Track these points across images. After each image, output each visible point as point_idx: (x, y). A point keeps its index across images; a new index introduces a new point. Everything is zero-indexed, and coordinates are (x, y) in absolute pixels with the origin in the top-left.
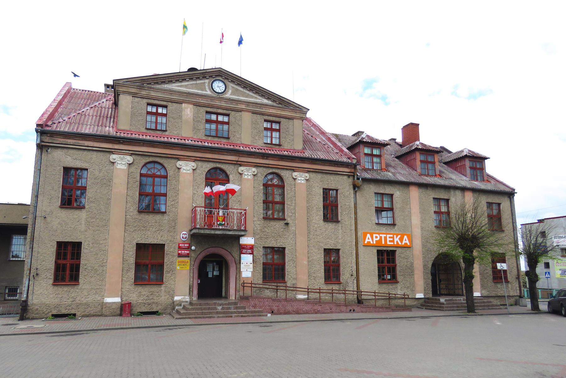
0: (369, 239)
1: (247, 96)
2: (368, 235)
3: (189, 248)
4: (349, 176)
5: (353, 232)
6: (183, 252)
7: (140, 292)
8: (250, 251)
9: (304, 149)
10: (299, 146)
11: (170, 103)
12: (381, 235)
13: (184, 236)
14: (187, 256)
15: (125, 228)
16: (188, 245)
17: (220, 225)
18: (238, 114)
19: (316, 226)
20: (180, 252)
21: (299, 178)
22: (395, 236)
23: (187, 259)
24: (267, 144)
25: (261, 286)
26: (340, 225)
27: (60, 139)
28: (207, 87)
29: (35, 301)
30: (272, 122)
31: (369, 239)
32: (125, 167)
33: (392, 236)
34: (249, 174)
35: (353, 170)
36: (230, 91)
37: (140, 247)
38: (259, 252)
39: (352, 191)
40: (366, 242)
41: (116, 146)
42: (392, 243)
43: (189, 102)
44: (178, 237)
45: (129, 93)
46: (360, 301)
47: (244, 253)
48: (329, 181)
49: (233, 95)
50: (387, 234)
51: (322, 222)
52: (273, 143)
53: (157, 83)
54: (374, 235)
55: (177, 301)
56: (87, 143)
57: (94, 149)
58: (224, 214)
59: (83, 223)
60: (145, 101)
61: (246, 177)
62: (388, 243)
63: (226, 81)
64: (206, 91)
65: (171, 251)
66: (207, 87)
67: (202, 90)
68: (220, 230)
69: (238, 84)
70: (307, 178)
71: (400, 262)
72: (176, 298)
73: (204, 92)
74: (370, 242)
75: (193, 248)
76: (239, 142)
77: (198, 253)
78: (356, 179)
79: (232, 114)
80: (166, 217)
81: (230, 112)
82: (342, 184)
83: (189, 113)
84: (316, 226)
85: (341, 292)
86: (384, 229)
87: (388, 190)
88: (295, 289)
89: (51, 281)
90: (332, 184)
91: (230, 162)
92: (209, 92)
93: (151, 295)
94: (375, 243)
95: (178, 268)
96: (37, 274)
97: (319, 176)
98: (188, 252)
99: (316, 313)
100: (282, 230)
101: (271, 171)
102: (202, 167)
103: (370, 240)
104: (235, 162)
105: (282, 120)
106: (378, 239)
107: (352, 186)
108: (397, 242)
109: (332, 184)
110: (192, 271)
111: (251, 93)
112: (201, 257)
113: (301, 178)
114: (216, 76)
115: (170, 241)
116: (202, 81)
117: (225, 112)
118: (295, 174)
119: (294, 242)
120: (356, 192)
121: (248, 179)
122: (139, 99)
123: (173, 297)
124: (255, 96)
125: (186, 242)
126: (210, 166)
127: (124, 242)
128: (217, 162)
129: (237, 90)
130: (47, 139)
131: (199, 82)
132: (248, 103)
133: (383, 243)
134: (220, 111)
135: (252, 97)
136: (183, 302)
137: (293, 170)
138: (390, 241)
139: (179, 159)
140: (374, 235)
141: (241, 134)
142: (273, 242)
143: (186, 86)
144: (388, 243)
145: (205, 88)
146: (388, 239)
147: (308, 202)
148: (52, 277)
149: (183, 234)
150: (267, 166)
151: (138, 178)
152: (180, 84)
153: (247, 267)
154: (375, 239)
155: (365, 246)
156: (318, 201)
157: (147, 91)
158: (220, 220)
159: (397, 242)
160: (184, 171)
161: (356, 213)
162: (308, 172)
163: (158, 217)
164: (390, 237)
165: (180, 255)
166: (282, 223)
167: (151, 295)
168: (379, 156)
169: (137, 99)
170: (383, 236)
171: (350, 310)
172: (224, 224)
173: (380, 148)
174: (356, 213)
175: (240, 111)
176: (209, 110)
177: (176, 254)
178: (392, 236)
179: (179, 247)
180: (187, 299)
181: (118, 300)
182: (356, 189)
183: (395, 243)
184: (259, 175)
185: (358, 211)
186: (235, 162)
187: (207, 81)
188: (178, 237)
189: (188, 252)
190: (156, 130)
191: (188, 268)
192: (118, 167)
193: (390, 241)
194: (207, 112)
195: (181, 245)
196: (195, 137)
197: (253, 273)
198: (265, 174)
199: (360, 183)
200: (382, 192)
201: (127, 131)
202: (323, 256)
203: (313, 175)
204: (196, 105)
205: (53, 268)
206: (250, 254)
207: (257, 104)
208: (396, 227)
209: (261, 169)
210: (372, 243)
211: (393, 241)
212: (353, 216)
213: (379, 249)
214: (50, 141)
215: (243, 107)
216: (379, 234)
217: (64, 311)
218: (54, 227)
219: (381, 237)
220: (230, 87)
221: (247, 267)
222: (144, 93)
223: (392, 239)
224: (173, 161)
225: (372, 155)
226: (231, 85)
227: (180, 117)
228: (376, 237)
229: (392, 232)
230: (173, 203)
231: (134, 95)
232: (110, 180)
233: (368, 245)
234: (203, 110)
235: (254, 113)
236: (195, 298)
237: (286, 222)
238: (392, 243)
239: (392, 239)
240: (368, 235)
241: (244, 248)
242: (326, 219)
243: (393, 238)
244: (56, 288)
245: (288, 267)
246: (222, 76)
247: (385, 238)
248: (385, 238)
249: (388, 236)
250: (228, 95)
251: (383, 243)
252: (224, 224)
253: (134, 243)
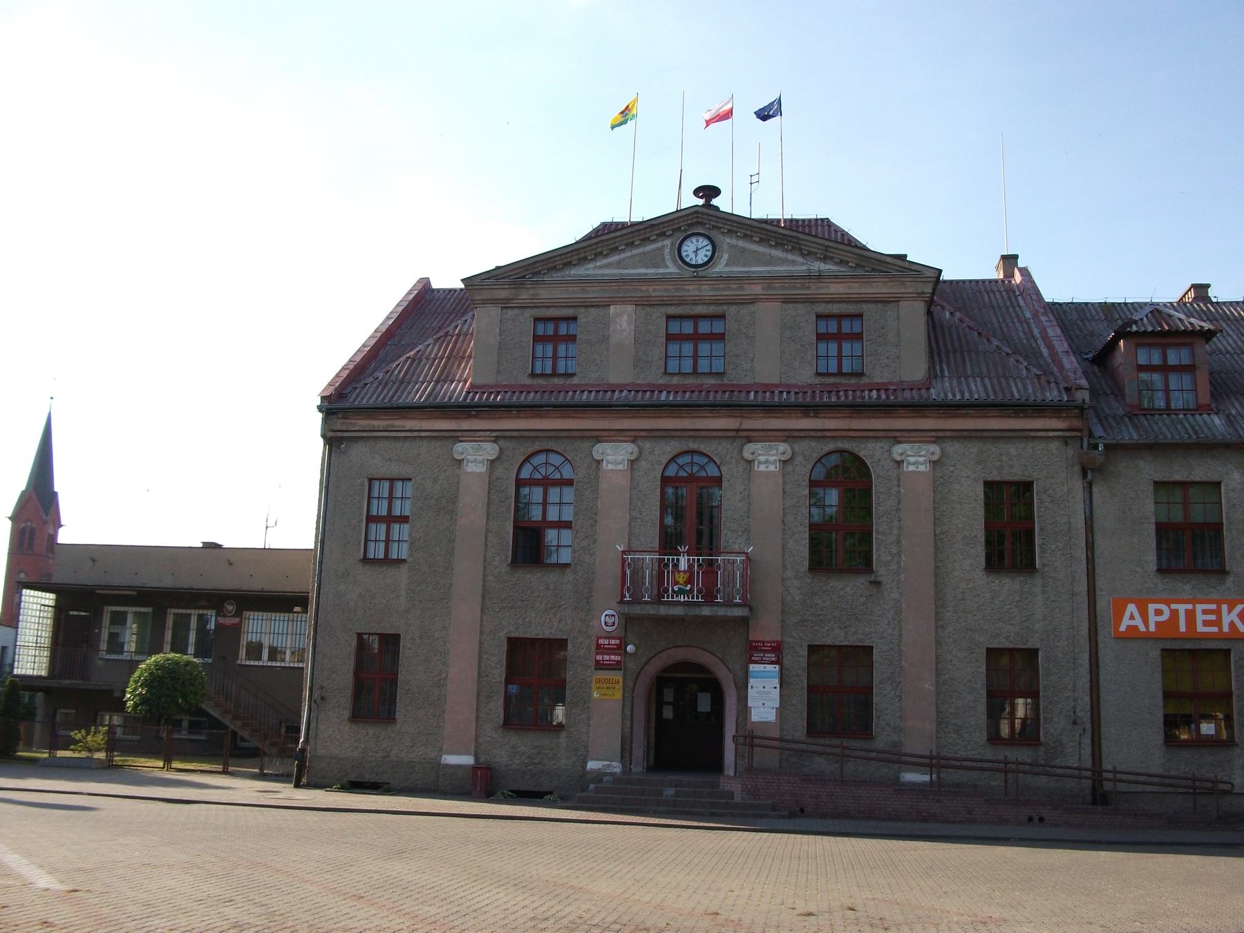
0: (1132, 617)
1: (770, 261)
2: (1131, 608)
3: (621, 648)
4: (1065, 441)
5: (1083, 599)
6: (607, 657)
7: (514, 747)
8: (772, 657)
9: (932, 376)
10: (914, 367)
11: (583, 310)
12: (1173, 606)
13: (610, 621)
14: (616, 666)
15: (483, 603)
16: (618, 642)
17: (681, 592)
18: (745, 311)
19: (963, 585)
20: (599, 658)
21: (912, 459)
22: (1224, 607)
23: (617, 676)
24: (828, 375)
25: (803, 746)
26: (1038, 581)
27: (360, 422)
28: (667, 257)
29: (321, 752)
30: (840, 317)
31: (1132, 617)
32: (482, 469)
33: (1213, 607)
34: (772, 458)
35: (1076, 423)
36: (726, 256)
37: (515, 645)
38: (798, 659)
39: (1078, 485)
40: (1123, 628)
41: (465, 425)
42: (1215, 629)
43: (623, 301)
44: (595, 623)
45: (494, 302)
46: (1100, 798)
47: (756, 662)
48: (1004, 458)
49: (734, 264)
50: (1194, 602)
51: (980, 577)
52: (845, 370)
53: (554, 268)
54: (1152, 607)
55: (592, 771)
56: (408, 424)
57: (423, 434)
58: (691, 566)
59: (403, 593)
60: (529, 313)
61: (762, 468)
62: (1200, 628)
63: (713, 234)
64: (667, 267)
65: (579, 653)
66: (667, 257)
67: (655, 266)
68: (679, 603)
69: (745, 236)
70: (935, 458)
71: (411, 671)
72: (592, 765)
73: (661, 271)
74: (1136, 627)
75: (630, 648)
76: (748, 381)
77: (643, 660)
78: (1085, 446)
79: (731, 311)
80: (569, 576)
81: (725, 307)
82: (1046, 464)
83: (624, 325)
84: (963, 585)
85: (1037, 769)
86: (1187, 587)
87: (1200, 470)
88: (899, 758)
89: (347, 714)
90: (1011, 466)
91: (720, 434)
92: (672, 269)
93: (539, 753)
94: (1152, 628)
95: (595, 695)
96: (322, 698)
97: (974, 448)
98: (618, 658)
99: (925, 820)
100: (863, 599)
101: (830, 446)
102: (652, 452)
103: (1138, 622)
104: (733, 434)
105: (866, 309)
106: (1165, 617)
107: (1077, 468)
108: (1232, 624)
109: (1011, 466)
110: (628, 704)
111: (777, 253)
112: (653, 669)
113: (916, 459)
114: (689, 225)
115: (580, 632)
116: (659, 245)
117: (712, 310)
118: (898, 450)
119: (896, 633)
120: (1090, 484)
121: (768, 474)
122: (516, 311)
123: (585, 763)
124: (790, 257)
125: (614, 634)
126: (672, 447)
127: (481, 633)
128: (690, 437)
129: (743, 250)
130: (339, 424)
131: (649, 248)
132: (768, 279)
133: (1183, 628)
134: (699, 310)
135: (783, 261)
136: (606, 774)
137: (896, 437)
138: (1206, 623)
139: (598, 440)
140: (1152, 607)
141: (753, 360)
142: (837, 631)
143: (618, 264)
144: (1200, 628)
145: (663, 259)
146: (1200, 618)
147: (936, 521)
148: (349, 705)
149: (607, 618)
150: (819, 434)
151: (512, 491)
152: (605, 261)
153: (764, 697)
154: (1153, 619)
155: (1121, 638)
156: (969, 517)
157: (531, 292)
158: (681, 580)
159: (1232, 624)
160: (610, 467)
161: (1090, 546)
162: (937, 440)
163: (552, 577)
164: (1205, 612)
165: (599, 666)
166: (861, 581)
167: (539, 753)
168: (1190, 369)
169: (510, 312)
170: (1182, 608)
171: (1030, 819)
172: (691, 591)
173: (1191, 345)
174: (1090, 546)
175: (753, 301)
176: (673, 310)
177: (592, 663)
178: (1213, 607)
179: (598, 646)
180: (616, 767)
181: (468, 760)
182: (1089, 476)
183: (1226, 629)
184: (799, 459)
185: (1098, 539)
186: (733, 434)
187: (668, 242)
188: (595, 623)
189: (618, 658)
190: (554, 374)
191: (618, 695)
192: (468, 470)
193: (1206, 623)
194: (669, 317)
195: (601, 641)
196: (640, 381)
197: (781, 711)
198: (816, 456)
199: (1101, 459)
200: (1178, 477)
201: (491, 387)
202: (983, 669)
203: (953, 447)
204: (643, 303)
205: (351, 686)
206: (772, 663)
207: (791, 277)
208: (1229, 581)
209: (801, 446)
210: (1142, 629)
211: (1218, 623)
212: (1081, 554)
213: (1169, 646)
214: (344, 428)
215: (757, 289)
216: (1167, 602)
217: (369, 777)
218: (352, 604)
219: (1174, 613)
220: (725, 247)
221: (764, 697)
222: (525, 296)
223: (1213, 617)
224: (585, 445)
225: (1165, 369)
226: (726, 241)
227: (605, 339)
228: (1158, 612)
229: (1214, 597)
230: (585, 543)
231: (505, 304)
232: (454, 500)
233: (1133, 635)
234: (658, 314)
235: (787, 301)
236: (638, 768)
237: (873, 578)
238: (1215, 629)
239: (1213, 617)
240: (1131, 608)
241: (756, 649)
242: (996, 561)
243: (1218, 612)
244: (354, 727)
245: (880, 699)
246: (703, 224)
247: (1191, 615)
248: (1191, 615)
249: (1199, 607)
250: (720, 268)
251: (1183, 628)
252: (691, 591)
253: (502, 635)
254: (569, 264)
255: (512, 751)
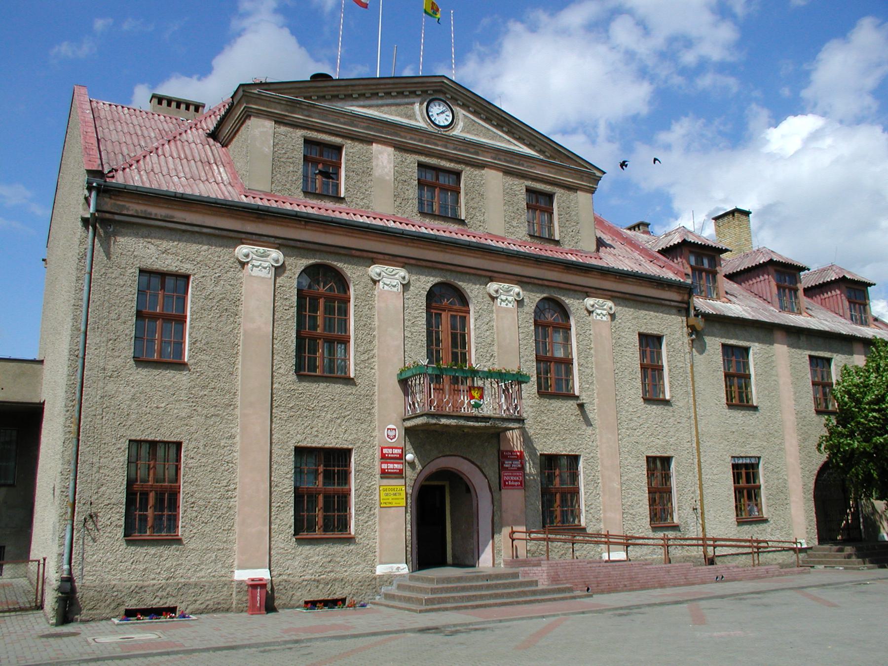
1: (494, 137)
6: (391, 466)
7: (307, 557)
13: (392, 433)
14: (399, 474)
16: (399, 451)
20: (384, 466)
21: (599, 311)
29: (88, 580)
34: (510, 298)
45: (268, 116)
57: (205, 230)
60: (300, 133)
70: (612, 312)
82: (672, 328)
83: (385, 162)
84: (631, 410)
92: (421, 124)
115: (364, 442)
121: (507, 310)
130: (109, 204)
132: (498, 152)
163: (338, 388)
165: (385, 474)
175: (482, 166)
177: (377, 471)
179: (383, 457)
192: (253, 274)
195: (385, 451)
196: (399, 215)
204: (401, 148)
226: (460, 112)
231: (280, 121)
234: (412, 160)
235: (507, 172)
237: (579, 402)
241: (506, 457)
246: (445, 93)
250: (457, 132)
254: (348, 97)
255: (309, 565)
